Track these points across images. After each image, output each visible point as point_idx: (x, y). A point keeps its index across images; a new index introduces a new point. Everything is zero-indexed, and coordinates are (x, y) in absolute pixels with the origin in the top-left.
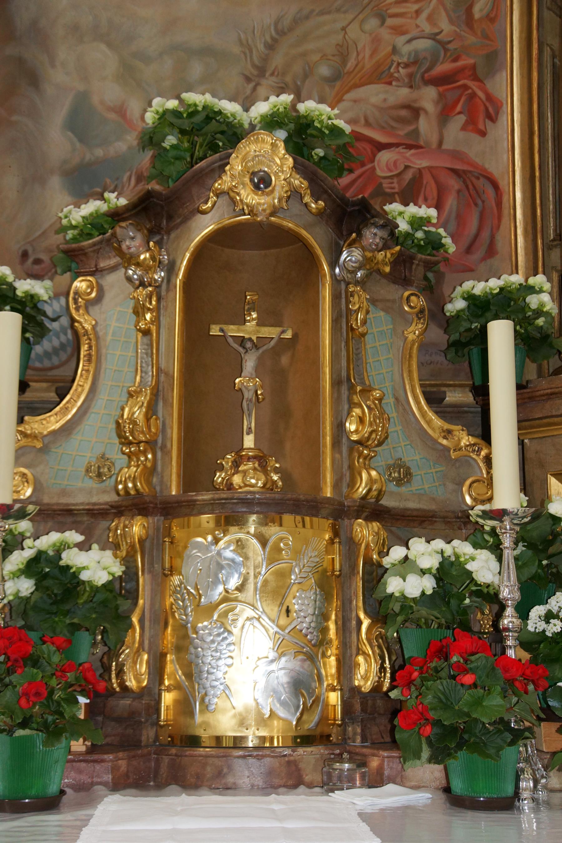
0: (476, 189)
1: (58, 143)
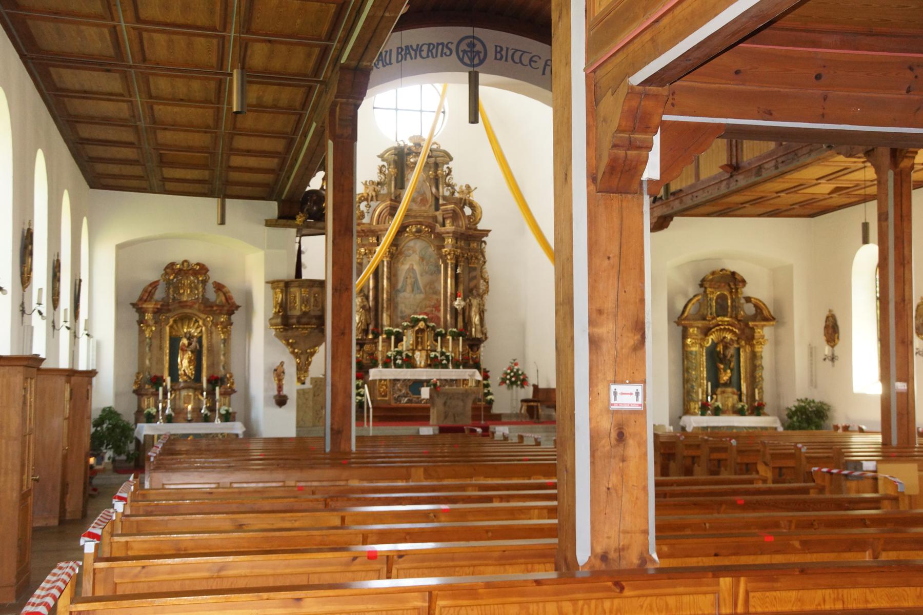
0: (439, 318)
1: (399, 314)
